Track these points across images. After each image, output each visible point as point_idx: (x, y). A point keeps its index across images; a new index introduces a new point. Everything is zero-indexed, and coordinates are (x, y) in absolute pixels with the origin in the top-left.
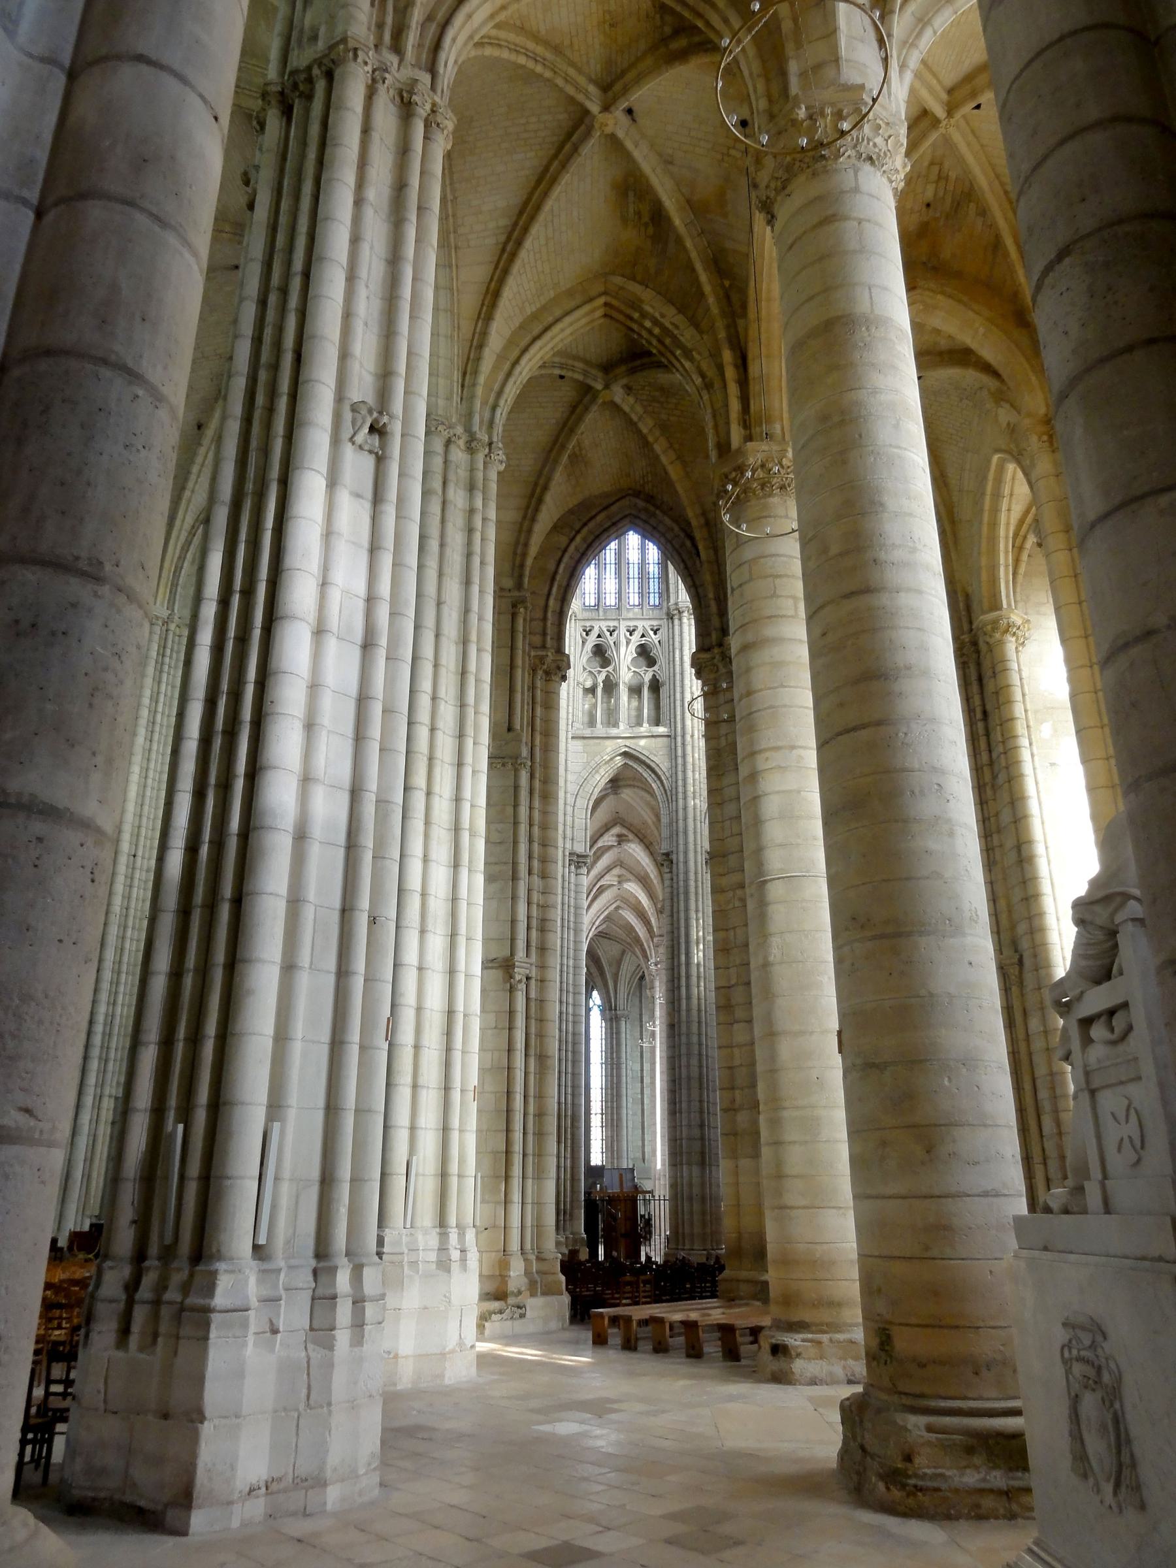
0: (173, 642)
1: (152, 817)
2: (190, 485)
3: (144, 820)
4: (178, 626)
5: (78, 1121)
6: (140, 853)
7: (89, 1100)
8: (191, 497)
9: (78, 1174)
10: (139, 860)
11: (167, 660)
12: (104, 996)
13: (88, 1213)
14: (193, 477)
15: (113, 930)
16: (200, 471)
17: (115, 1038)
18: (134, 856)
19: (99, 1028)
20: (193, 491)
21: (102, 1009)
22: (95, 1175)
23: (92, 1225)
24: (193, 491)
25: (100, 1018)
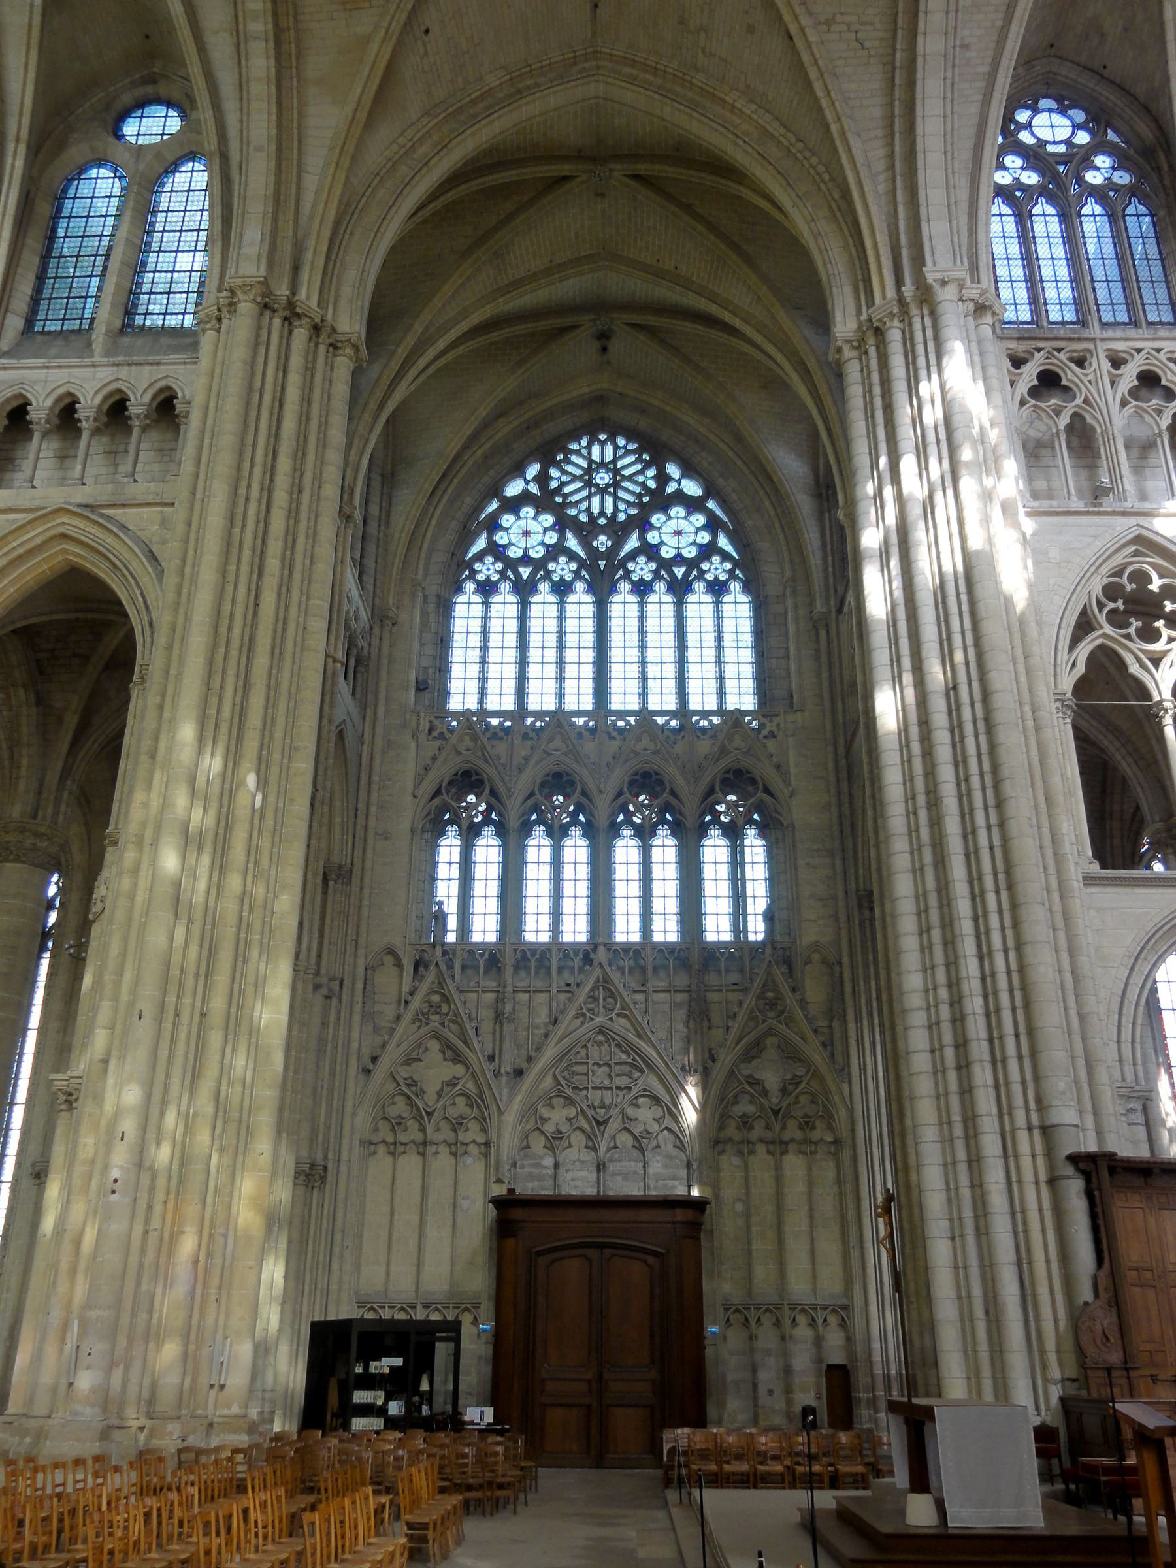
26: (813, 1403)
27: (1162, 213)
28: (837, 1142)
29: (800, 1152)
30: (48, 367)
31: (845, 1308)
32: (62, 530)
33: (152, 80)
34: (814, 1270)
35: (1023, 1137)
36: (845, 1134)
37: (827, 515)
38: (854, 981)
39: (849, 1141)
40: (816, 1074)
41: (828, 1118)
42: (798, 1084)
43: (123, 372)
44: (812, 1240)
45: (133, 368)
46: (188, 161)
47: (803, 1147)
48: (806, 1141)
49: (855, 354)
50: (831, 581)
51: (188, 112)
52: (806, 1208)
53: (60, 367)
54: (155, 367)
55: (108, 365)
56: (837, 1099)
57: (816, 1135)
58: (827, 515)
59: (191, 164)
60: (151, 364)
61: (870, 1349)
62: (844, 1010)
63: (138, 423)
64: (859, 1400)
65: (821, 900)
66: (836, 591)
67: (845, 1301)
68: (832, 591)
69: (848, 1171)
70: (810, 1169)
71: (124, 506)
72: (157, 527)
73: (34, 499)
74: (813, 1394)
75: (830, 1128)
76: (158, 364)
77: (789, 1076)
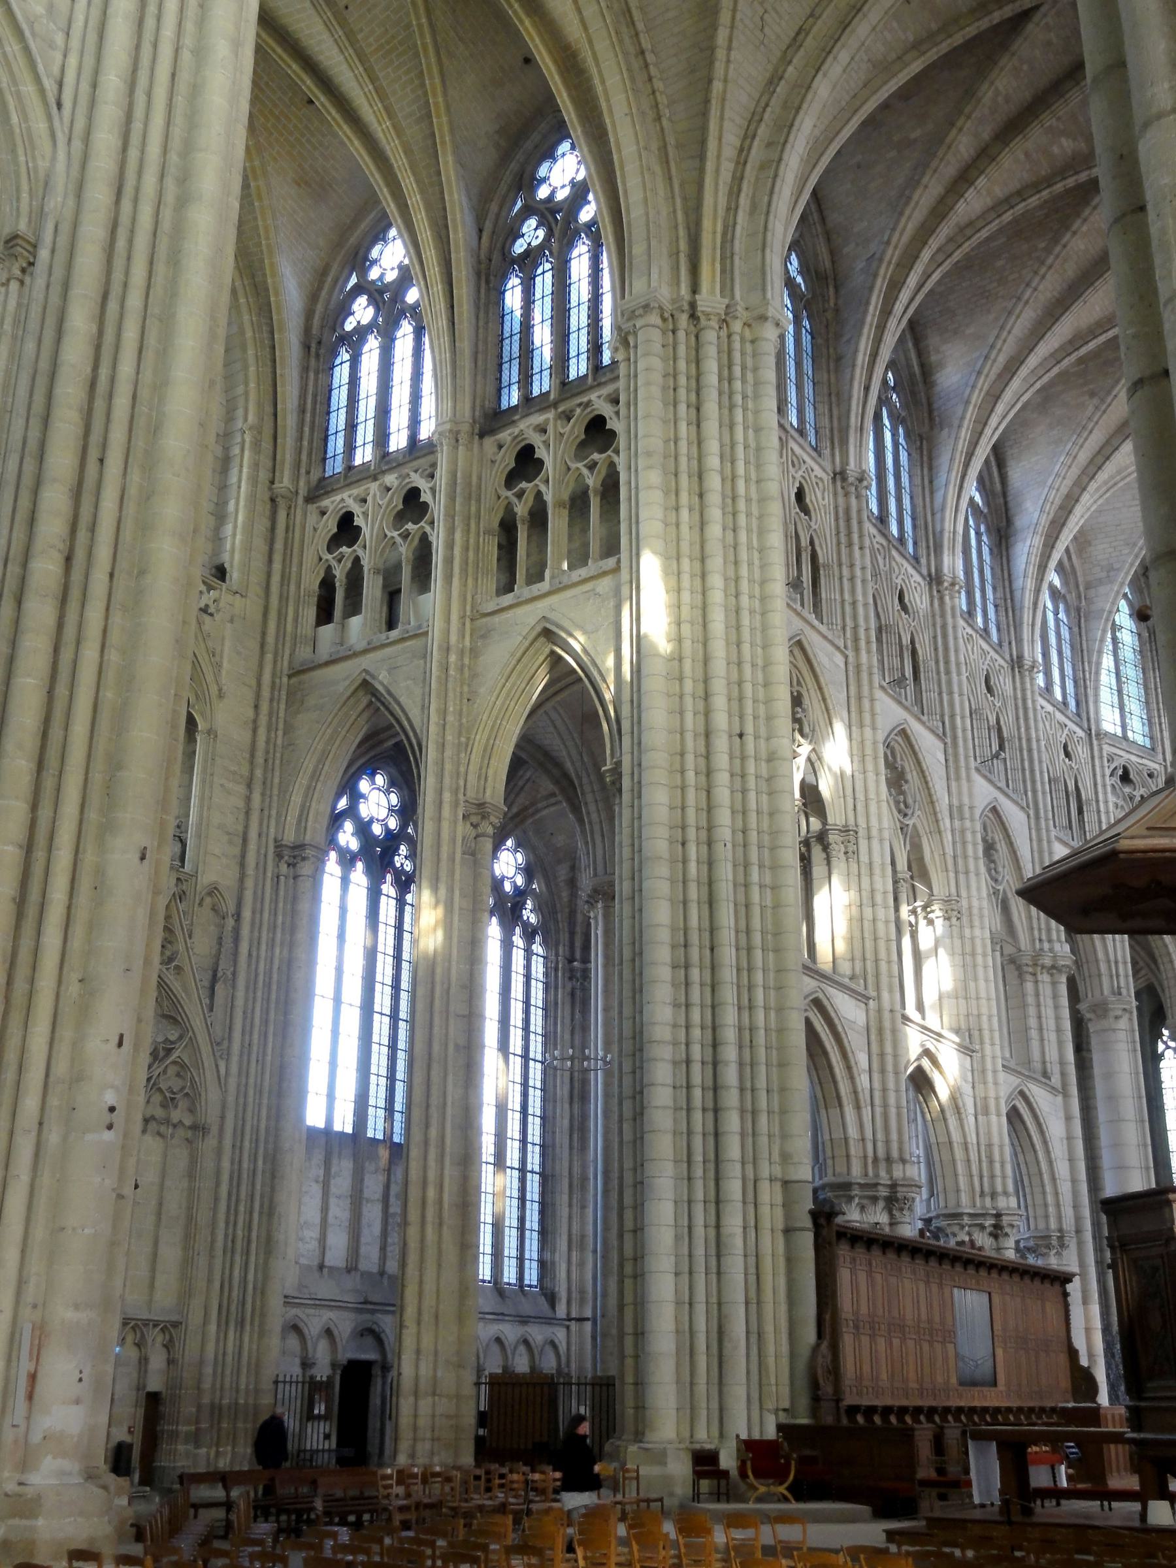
0: (743, 354)
1: (760, 662)
2: (719, 68)
3: (747, 670)
4: (747, 325)
5: (723, 1231)
6: (749, 729)
7: (734, 1188)
8: (725, 91)
9: (738, 1328)
10: (749, 740)
11: (738, 385)
12: (729, 994)
13: (770, 1405)
14: (720, 54)
15: (725, 872)
16: (730, 40)
17: (762, 1069)
18: (741, 736)
19: (730, 1053)
20: (725, 81)
21: (730, 1017)
22: (769, 1328)
23: (780, 1428)
24: (725, 81)
25: (730, 1035)
26: (127, 1438)
27: (820, 341)
28: (199, 1129)
29: (159, 1134)
31: (176, 1325)
34: (153, 1279)
35: (764, 1186)
36: (211, 1116)
37: (312, 375)
38: (255, 943)
39: (214, 1130)
40: (193, 1044)
41: (193, 1097)
42: (169, 1051)
44: (156, 1243)
47: (163, 1129)
48: (167, 1121)
49: (659, 321)
50: (304, 457)
52: (154, 1202)
56: (210, 1075)
57: (176, 1115)
58: (312, 375)
61: (200, 1374)
62: (234, 974)
64: (174, 1435)
65: (228, 834)
66: (308, 473)
67: (174, 1318)
68: (303, 471)
69: (209, 1164)
70: (165, 1156)
74: (125, 1429)
75: (192, 1111)
77: (160, 1039)
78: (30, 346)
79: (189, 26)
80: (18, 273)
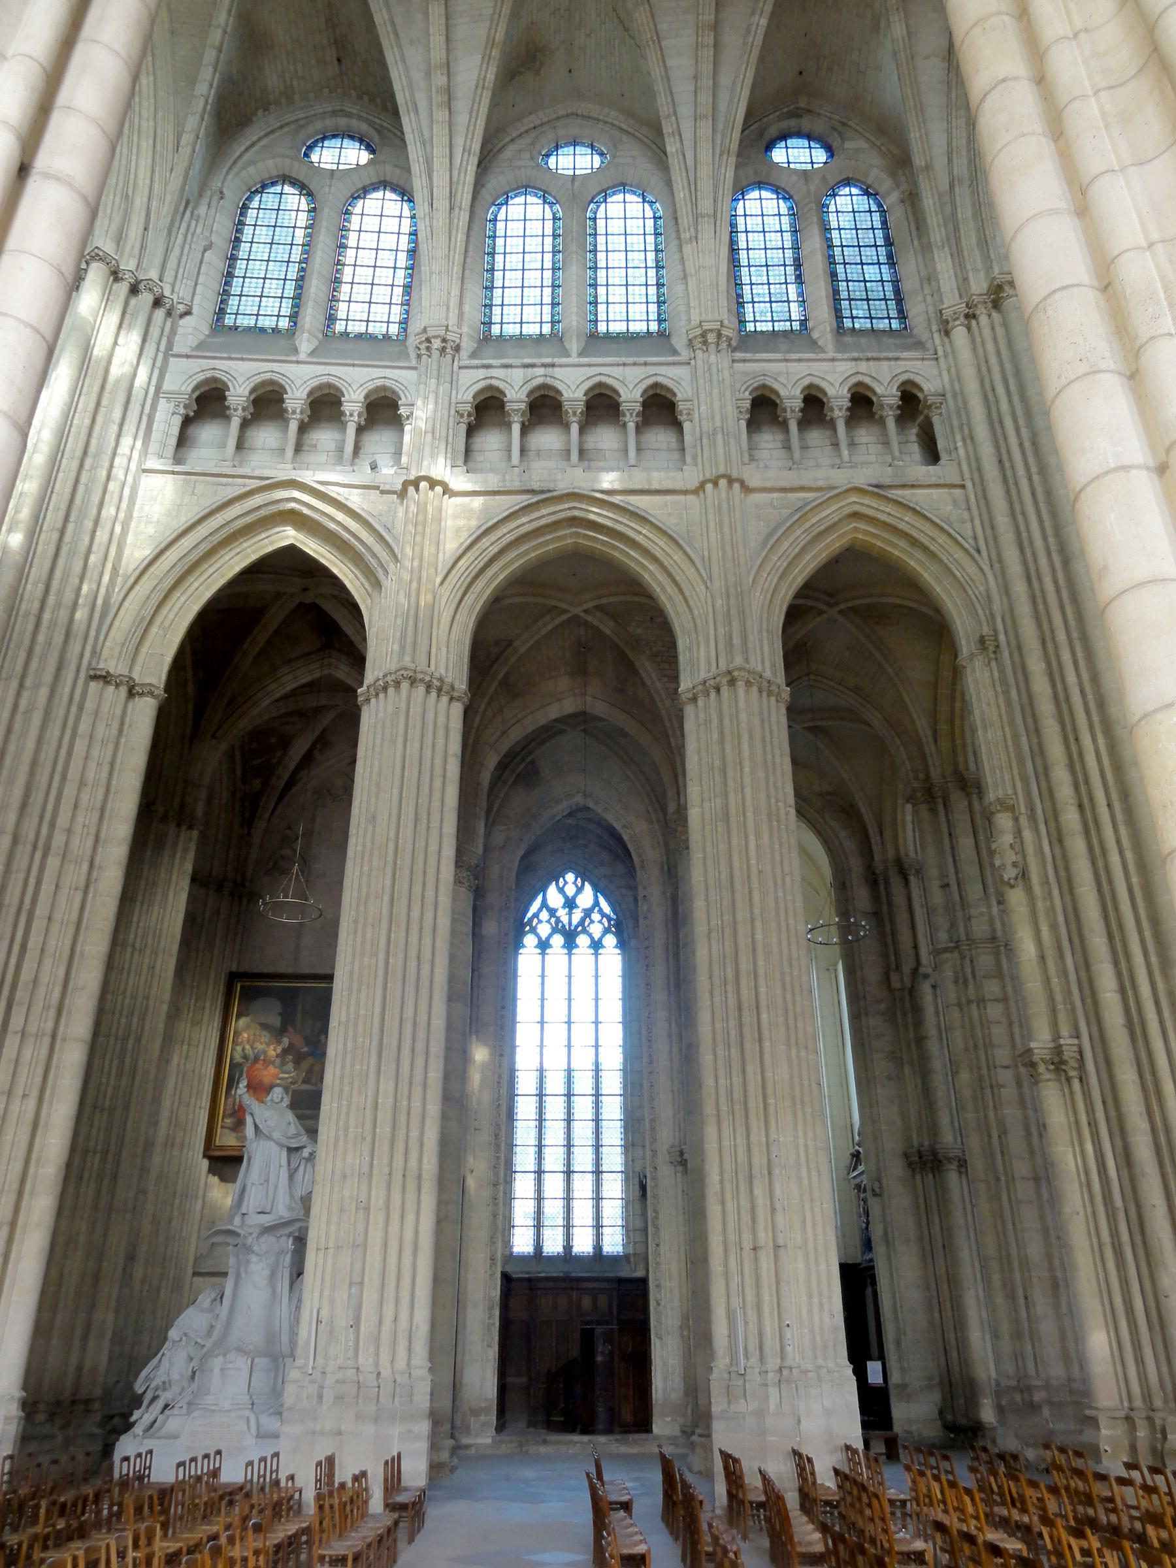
30: (787, 361)
32: (857, 508)
33: (796, 114)
43: (863, 367)
45: (871, 363)
46: (845, 186)
51: (835, 144)
53: (800, 360)
54: (892, 363)
55: (846, 360)
59: (847, 189)
60: (889, 359)
63: (891, 413)
71: (913, 486)
72: (950, 507)
73: (816, 480)
76: (897, 359)
78: (1014, 692)
79: (1031, 460)
80: (992, 656)
